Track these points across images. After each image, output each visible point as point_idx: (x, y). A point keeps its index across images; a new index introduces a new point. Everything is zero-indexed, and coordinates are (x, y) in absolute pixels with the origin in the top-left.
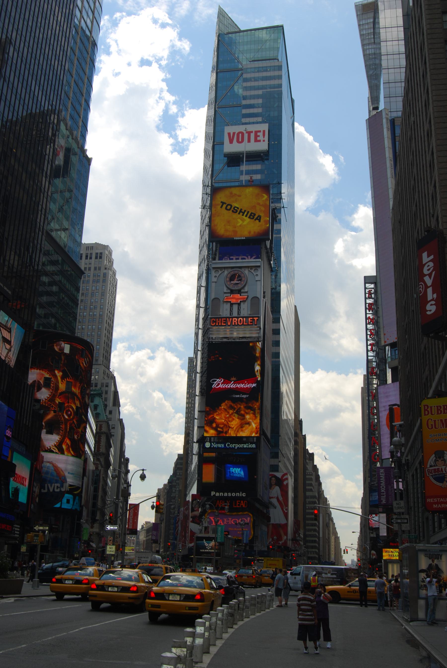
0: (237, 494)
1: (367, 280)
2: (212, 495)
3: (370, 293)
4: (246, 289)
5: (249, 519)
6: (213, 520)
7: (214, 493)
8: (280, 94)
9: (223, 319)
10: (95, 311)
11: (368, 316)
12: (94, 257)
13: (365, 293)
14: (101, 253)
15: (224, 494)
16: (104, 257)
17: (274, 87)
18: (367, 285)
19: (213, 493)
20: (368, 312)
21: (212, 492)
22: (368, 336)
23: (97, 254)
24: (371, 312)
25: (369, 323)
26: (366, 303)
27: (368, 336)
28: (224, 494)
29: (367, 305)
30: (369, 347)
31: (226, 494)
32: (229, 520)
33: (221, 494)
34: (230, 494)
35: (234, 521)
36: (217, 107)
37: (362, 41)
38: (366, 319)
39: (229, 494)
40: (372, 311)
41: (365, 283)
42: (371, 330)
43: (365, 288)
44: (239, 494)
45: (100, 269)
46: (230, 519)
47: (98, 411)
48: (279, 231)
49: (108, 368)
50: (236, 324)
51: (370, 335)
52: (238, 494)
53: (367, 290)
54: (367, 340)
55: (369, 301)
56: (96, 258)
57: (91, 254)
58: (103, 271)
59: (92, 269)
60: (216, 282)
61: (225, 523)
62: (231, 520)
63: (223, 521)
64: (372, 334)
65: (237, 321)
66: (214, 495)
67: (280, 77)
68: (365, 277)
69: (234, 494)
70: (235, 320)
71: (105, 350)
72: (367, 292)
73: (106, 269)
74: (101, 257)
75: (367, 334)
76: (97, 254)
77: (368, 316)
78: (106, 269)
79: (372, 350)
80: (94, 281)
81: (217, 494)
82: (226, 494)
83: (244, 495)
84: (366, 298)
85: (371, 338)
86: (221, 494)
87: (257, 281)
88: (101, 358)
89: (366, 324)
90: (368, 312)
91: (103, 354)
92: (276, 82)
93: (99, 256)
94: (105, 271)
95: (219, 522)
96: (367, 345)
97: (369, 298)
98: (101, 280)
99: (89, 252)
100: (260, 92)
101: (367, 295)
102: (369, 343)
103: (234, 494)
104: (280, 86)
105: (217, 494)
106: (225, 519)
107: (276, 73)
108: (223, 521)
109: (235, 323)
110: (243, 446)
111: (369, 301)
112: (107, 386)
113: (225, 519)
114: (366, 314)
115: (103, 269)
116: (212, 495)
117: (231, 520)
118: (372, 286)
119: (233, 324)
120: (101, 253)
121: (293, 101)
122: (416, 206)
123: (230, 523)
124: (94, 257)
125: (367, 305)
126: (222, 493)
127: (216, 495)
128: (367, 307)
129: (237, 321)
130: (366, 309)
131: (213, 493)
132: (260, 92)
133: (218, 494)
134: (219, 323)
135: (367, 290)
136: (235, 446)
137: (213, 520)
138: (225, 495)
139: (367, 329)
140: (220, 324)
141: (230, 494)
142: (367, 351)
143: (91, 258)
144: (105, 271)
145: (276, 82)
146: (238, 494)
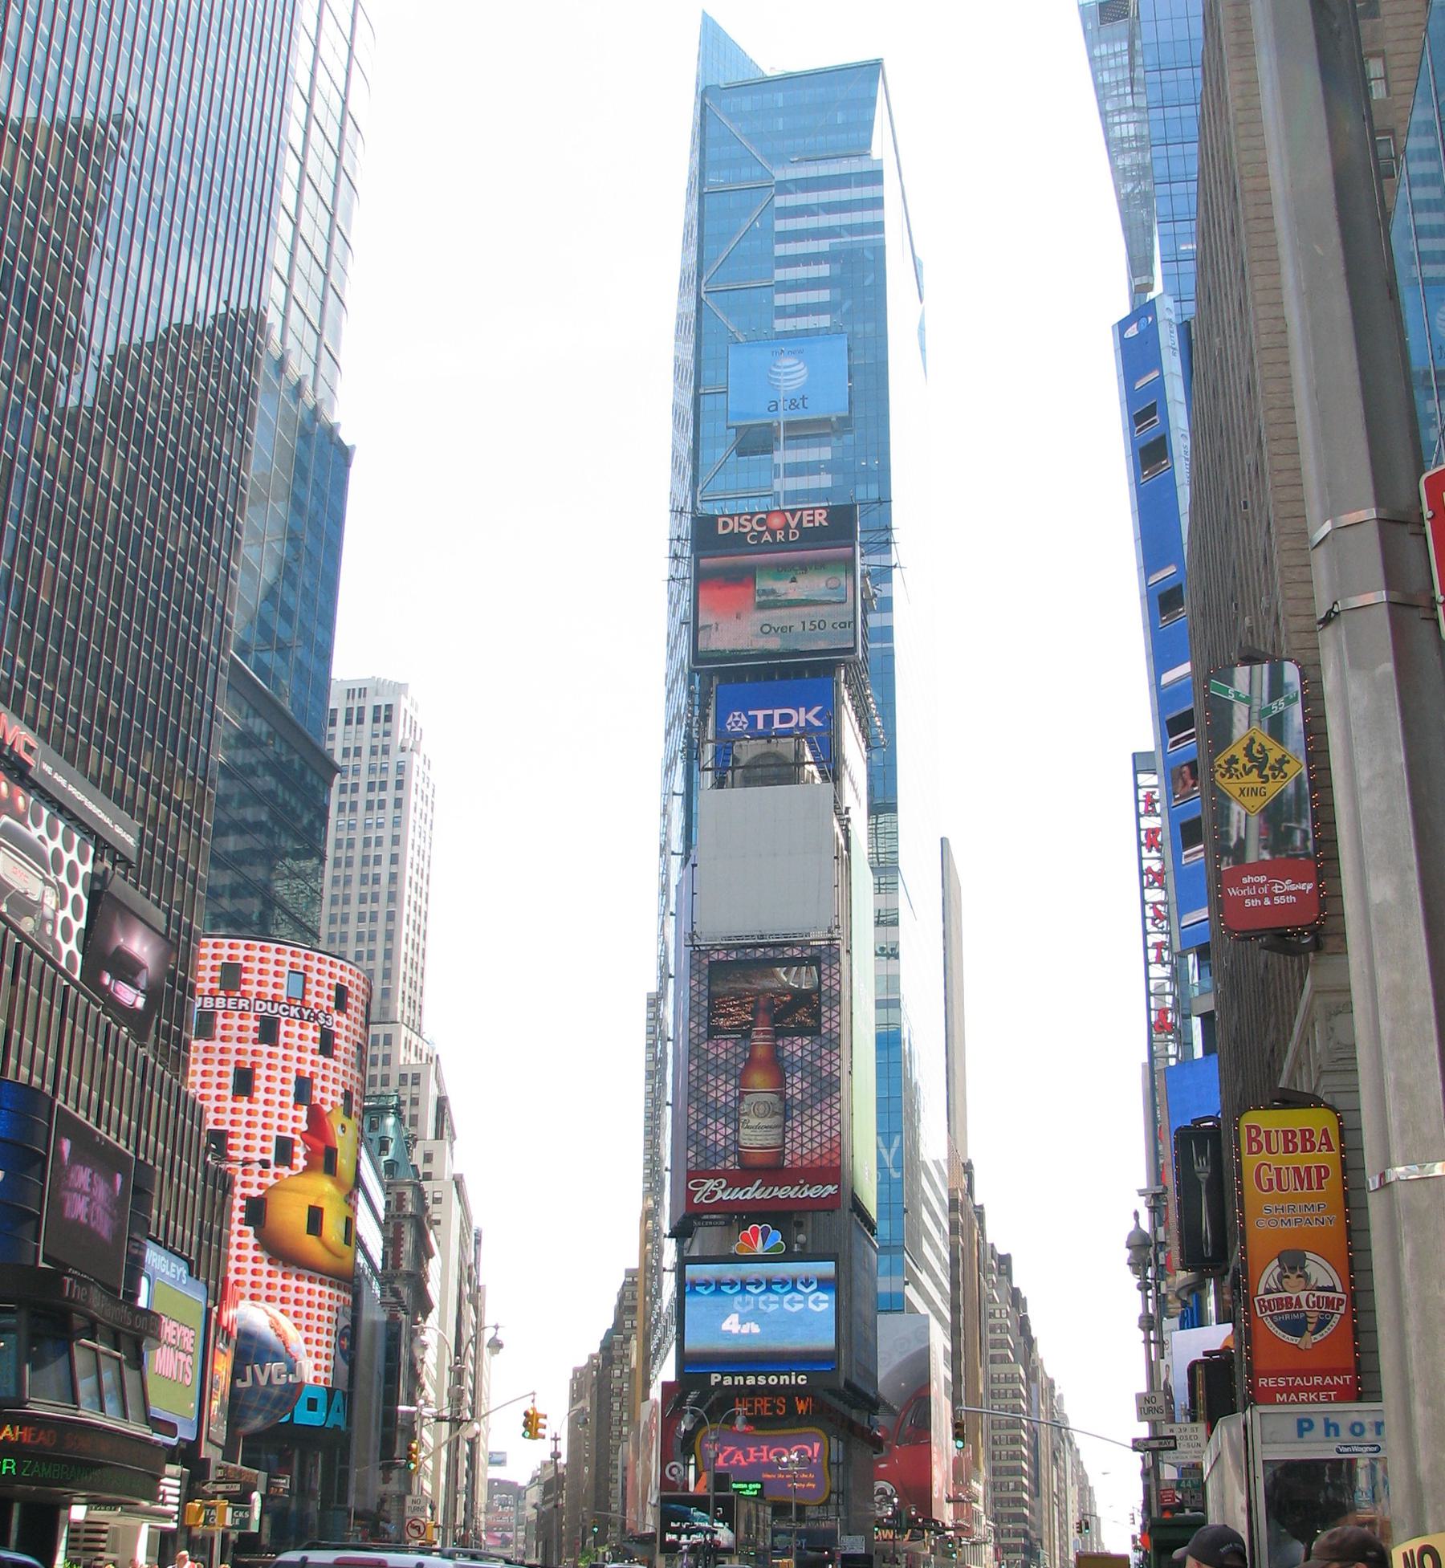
1: (1141, 763)
3: (1150, 801)
5: (817, 1446)
8: (879, 251)
10: (377, 870)
11: (1146, 864)
13: (1137, 801)
14: (389, 707)
16: (399, 717)
17: (862, 229)
18: (1143, 779)
21: (713, 1376)
22: (1149, 922)
23: (377, 708)
24: (1154, 853)
25: (1150, 885)
26: (1139, 830)
27: (1149, 922)
29: (1143, 833)
30: (1152, 954)
36: (703, 289)
37: (1101, 101)
38: (1142, 873)
40: (1159, 851)
41: (1136, 773)
42: (1155, 904)
43: (1137, 787)
45: (386, 751)
46: (765, 1448)
48: (887, 633)
51: (1154, 920)
54: (1146, 933)
56: (376, 720)
57: (361, 709)
58: (395, 757)
61: (752, 1459)
63: (746, 1456)
64: (1158, 916)
67: (877, 203)
69: (773, 1380)
72: (1141, 797)
73: (403, 749)
74: (388, 719)
75: (1144, 917)
76: (377, 708)
77: (1146, 864)
78: (403, 749)
79: (1160, 960)
81: (728, 1381)
83: (802, 1380)
84: (1138, 816)
85: (1155, 925)
89: (1142, 888)
92: (867, 217)
93: (385, 715)
94: (402, 757)
96: (1146, 948)
97: (1148, 813)
99: (355, 704)
100: (824, 245)
101: (1142, 806)
102: (1151, 940)
104: (879, 227)
105: (728, 1381)
106: (752, 1450)
107: (867, 192)
108: (746, 1456)
111: (1149, 823)
112: (416, 1083)
114: (1141, 859)
115: (394, 750)
120: (389, 707)
121: (917, 266)
122: (1234, 577)
123: (765, 1459)
125: (1143, 833)
128: (1143, 839)
130: (1140, 844)
131: (715, 1378)
132: (824, 245)
135: (1142, 793)
139: (1144, 903)
141: (762, 1380)
142: (1147, 964)
143: (360, 721)
144: (402, 757)
145: (867, 217)
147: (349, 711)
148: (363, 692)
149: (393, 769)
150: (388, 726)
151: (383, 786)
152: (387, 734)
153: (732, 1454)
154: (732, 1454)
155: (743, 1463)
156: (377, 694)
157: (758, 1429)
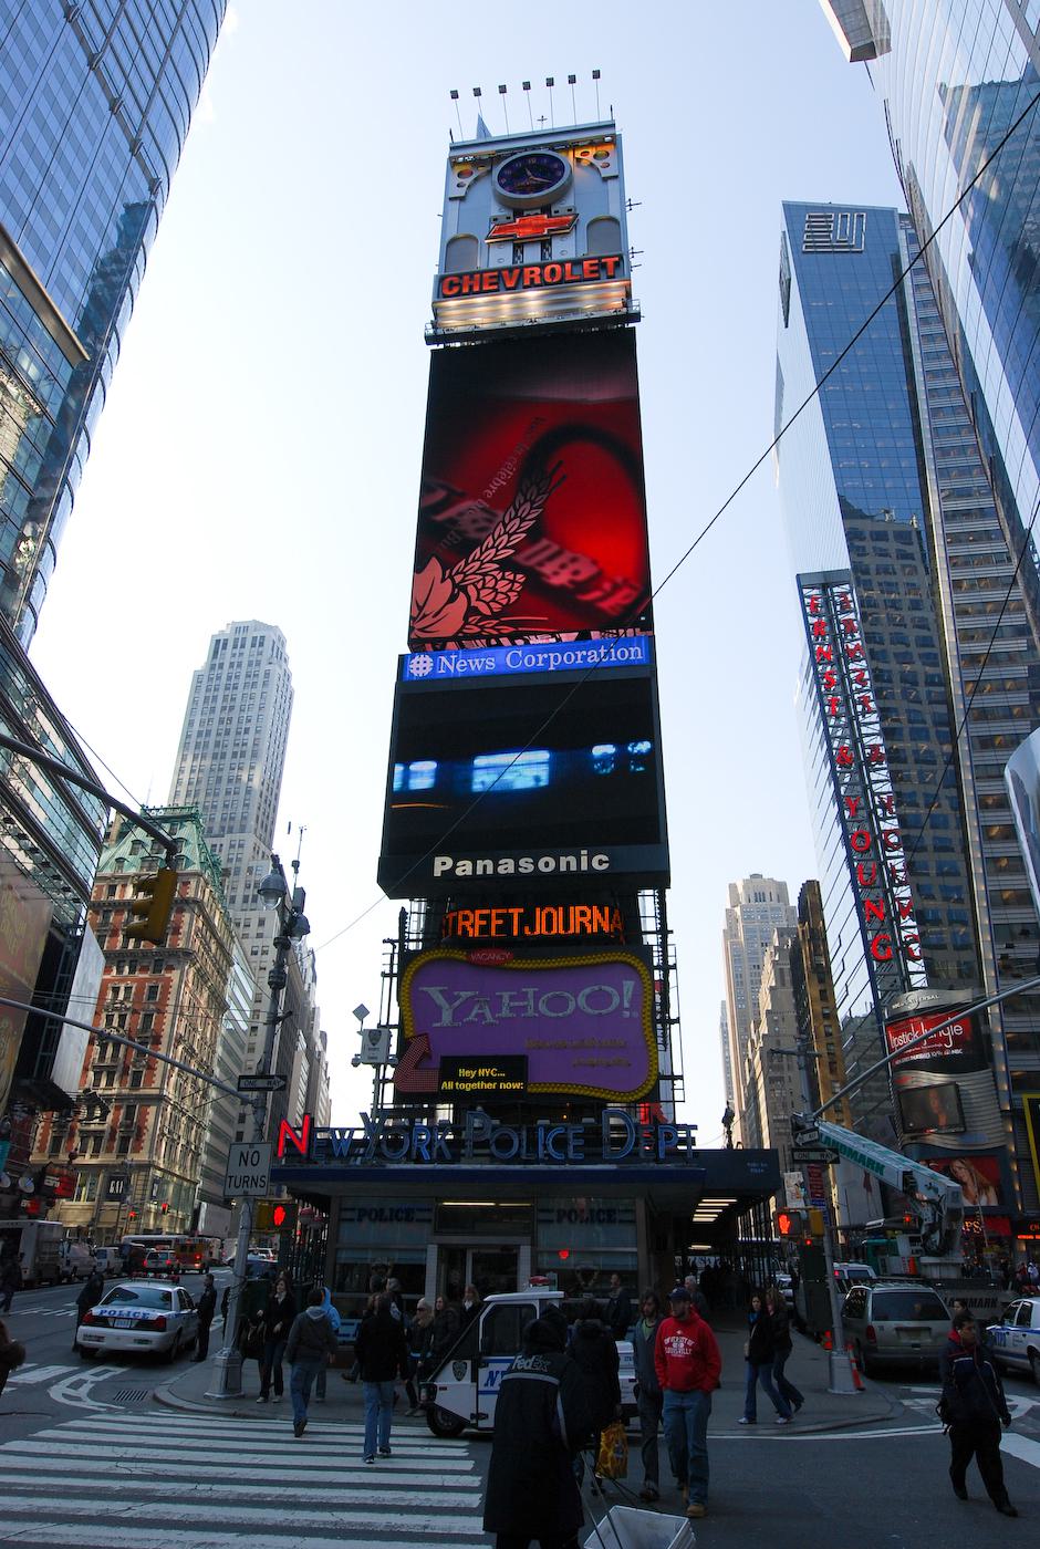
0: (563, 860)
2: (437, 873)
3: (814, 606)
4: (569, 202)
5: (629, 986)
6: (440, 1000)
7: (449, 862)
9: (485, 275)
10: (246, 736)
12: (248, 643)
13: (804, 606)
15: (496, 866)
18: (805, 591)
19: (442, 864)
21: (438, 861)
23: (255, 638)
28: (496, 866)
31: (507, 866)
32: (524, 997)
33: (485, 866)
34: (526, 865)
35: (550, 1004)
39: (522, 862)
41: (801, 588)
43: (802, 597)
44: (572, 859)
46: (531, 991)
49: (270, 847)
50: (537, 282)
52: (568, 862)
53: (807, 601)
55: (812, 620)
56: (253, 645)
57: (244, 639)
58: (264, 667)
59: (245, 665)
60: (462, 199)
61: (505, 1013)
62: (537, 997)
65: (541, 275)
66: (449, 874)
69: (547, 864)
70: (532, 272)
71: (262, 810)
74: (261, 644)
76: (255, 638)
81: (465, 868)
82: (507, 866)
86: (485, 866)
87: (605, 180)
88: (253, 823)
91: (258, 817)
95: (475, 1011)
98: (260, 683)
101: (808, 609)
103: (547, 864)
105: (465, 868)
106: (506, 995)
108: (496, 1006)
109: (532, 280)
110: (584, 658)
111: (812, 620)
113: (506, 995)
116: (437, 873)
117: (537, 997)
118: (815, 592)
119: (527, 283)
120: (262, 638)
123: (530, 1012)
124: (248, 643)
126: (489, 863)
127: (459, 872)
129: (541, 275)
133: (469, 864)
134: (471, 287)
135: (807, 601)
136: (547, 661)
137: (440, 1000)
138: (501, 870)
140: (476, 289)
141: (526, 865)
143: (243, 646)
146: (568, 862)
147: (236, 640)
148: (246, 629)
149: (262, 674)
150: (261, 649)
151: (254, 685)
152: (260, 654)
153: (468, 1005)
154: (468, 1005)
155: (490, 1018)
156: (255, 630)
157: (519, 957)
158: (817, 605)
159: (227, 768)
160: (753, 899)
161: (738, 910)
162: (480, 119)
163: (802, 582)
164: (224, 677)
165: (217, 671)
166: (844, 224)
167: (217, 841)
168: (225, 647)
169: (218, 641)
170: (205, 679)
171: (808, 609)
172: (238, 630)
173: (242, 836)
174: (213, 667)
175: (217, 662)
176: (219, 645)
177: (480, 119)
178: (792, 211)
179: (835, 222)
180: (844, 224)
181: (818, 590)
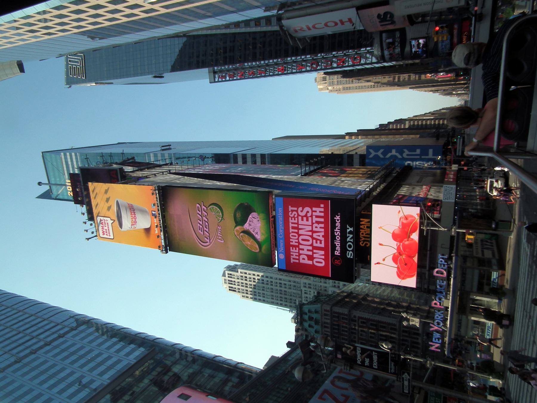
3: (223, 77)
18: (216, 80)
20: (235, 78)
23: (228, 277)
41: (215, 82)
43: (218, 81)
47: (313, 310)
53: (220, 80)
55: (228, 78)
57: (229, 281)
68: (210, 83)
76: (228, 277)
80: (246, 280)
84: (226, 81)
90: (235, 78)
101: (224, 80)
111: (228, 78)
118: (217, 76)
135: (220, 80)
143: (231, 281)
147: (229, 283)
158: (222, 76)
159: (276, 288)
160: (325, 82)
161: (330, 88)
162: (37, 197)
163: (213, 81)
164: (243, 288)
165: (241, 290)
166: (73, 62)
167: (303, 292)
168: (232, 287)
169: (230, 290)
170: (243, 294)
171: (224, 80)
172: (225, 283)
173: (302, 283)
174: (239, 292)
175: (237, 290)
176: (232, 289)
177: (37, 197)
178: (70, 82)
179: (72, 65)
180: (73, 62)
181: (218, 76)
